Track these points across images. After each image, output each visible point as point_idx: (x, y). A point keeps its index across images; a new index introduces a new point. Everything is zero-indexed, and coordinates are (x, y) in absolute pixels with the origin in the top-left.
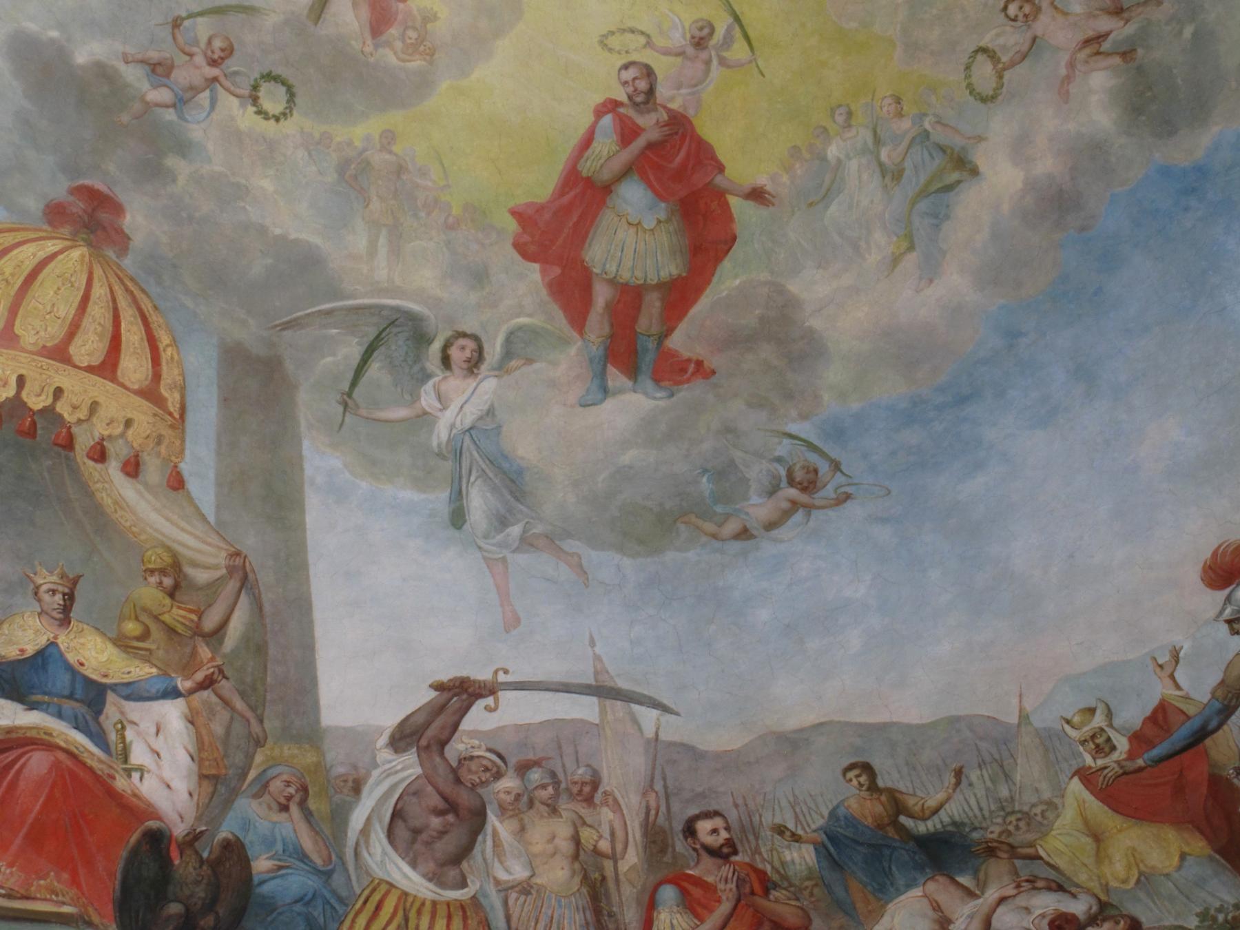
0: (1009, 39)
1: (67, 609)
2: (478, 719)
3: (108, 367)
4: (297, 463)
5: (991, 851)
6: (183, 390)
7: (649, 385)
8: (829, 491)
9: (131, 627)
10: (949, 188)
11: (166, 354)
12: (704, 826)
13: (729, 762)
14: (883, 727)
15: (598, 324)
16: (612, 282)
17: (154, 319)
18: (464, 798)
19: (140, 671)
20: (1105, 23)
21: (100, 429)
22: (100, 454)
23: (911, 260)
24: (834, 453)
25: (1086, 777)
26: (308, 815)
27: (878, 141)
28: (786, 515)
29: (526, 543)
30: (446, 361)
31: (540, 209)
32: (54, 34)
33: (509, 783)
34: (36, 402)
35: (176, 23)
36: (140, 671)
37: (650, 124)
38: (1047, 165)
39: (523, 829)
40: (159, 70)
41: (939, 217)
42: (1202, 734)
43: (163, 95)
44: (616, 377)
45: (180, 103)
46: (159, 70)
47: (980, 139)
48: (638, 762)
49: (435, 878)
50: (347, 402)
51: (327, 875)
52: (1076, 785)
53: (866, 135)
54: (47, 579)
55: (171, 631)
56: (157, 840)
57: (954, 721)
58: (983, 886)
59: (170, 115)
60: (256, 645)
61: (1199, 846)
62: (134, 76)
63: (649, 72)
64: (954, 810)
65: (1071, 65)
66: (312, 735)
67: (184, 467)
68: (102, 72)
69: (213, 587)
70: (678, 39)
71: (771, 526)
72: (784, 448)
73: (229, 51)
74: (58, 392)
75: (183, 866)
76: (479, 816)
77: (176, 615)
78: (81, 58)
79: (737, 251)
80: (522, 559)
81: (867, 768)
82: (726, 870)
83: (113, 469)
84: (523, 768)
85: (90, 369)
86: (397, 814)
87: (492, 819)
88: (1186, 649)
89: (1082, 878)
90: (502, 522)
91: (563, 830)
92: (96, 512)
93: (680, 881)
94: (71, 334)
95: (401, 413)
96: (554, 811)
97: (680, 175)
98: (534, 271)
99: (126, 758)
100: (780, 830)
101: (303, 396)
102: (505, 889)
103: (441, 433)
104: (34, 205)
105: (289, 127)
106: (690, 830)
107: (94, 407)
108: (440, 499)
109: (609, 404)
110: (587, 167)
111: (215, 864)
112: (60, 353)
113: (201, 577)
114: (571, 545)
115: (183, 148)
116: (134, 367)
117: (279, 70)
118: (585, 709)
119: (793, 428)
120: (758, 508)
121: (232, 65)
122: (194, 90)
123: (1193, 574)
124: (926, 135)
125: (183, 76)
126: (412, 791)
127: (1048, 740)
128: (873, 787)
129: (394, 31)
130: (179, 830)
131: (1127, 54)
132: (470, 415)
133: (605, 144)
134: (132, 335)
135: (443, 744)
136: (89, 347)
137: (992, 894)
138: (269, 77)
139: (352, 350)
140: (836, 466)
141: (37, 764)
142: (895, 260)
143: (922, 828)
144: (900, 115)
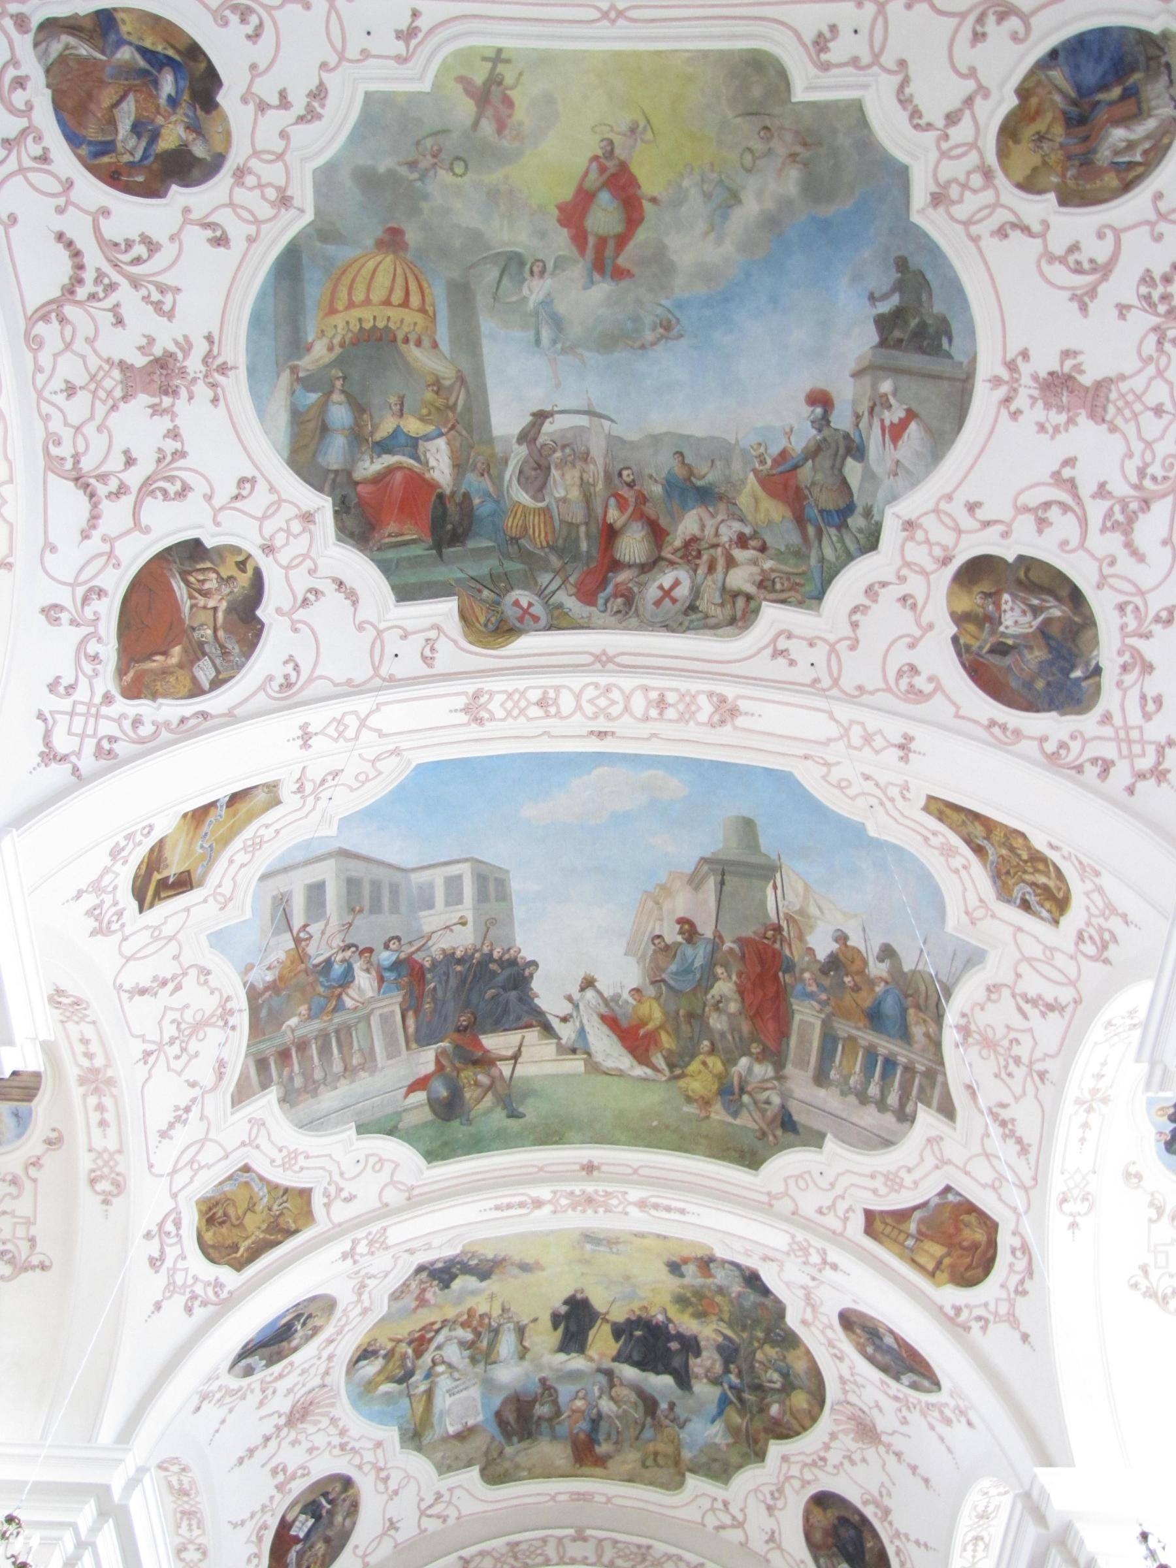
0: (758, 146)
1: (401, 410)
2: (548, 427)
3: (405, 303)
4: (477, 328)
5: (721, 498)
6: (433, 305)
7: (608, 278)
8: (675, 332)
9: (425, 411)
10: (730, 207)
11: (427, 291)
12: (625, 473)
13: (633, 445)
14: (689, 437)
15: (590, 252)
16: (596, 235)
17: (421, 277)
18: (543, 462)
19: (430, 429)
20: (798, 149)
21: (406, 329)
22: (406, 341)
23: (712, 236)
24: (678, 315)
25: (755, 471)
26: (490, 476)
27: (703, 181)
28: (659, 340)
29: (564, 351)
30: (532, 273)
31: (567, 204)
32: (370, 162)
33: (558, 454)
34: (381, 324)
35: (418, 143)
36: (430, 429)
37: (611, 166)
38: (770, 205)
39: (563, 475)
40: (412, 165)
41: (725, 217)
42: (796, 467)
43: (415, 176)
44: (596, 276)
45: (422, 178)
46: (412, 165)
47: (744, 188)
48: (603, 444)
49: (534, 498)
50: (495, 298)
51: (497, 502)
52: (751, 475)
53: (698, 178)
54: (393, 400)
55: (438, 409)
56: (441, 497)
57: (713, 438)
58: (717, 513)
59: (419, 184)
60: (468, 408)
61: (789, 514)
62: (403, 171)
63: (611, 143)
64: (710, 478)
65: (784, 164)
66: (489, 440)
67: (438, 338)
68: (391, 173)
69: (451, 387)
70: (624, 127)
71: (653, 344)
72: (659, 311)
73: (440, 150)
74: (389, 319)
75: (451, 508)
76: (549, 468)
77: (440, 402)
78: (382, 169)
79: (645, 224)
80: (562, 358)
81: (681, 454)
82: (632, 493)
83: (412, 346)
84: (564, 447)
85: (400, 306)
86: (521, 472)
87: (553, 471)
88: (796, 427)
89: (750, 518)
90: (554, 342)
91: (577, 474)
92: (407, 364)
93: (616, 496)
94: (391, 290)
95: (514, 299)
96: (574, 466)
97: (623, 188)
98: (565, 232)
99: (427, 462)
100: (651, 477)
101: (479, 298)
102: (558, 500)
103: (531, 305)
104: (370, 242)
105: (466, 178)
106: (620, 475)
107: (402, 321)
108: (531, 334)
109: (594, 288)
110: (587, 185)
111: (460, 505)
112: (387, 303)
113: (447, 383)
114: (580, 350)
115: (425, 197)
116: (415, 300)
117: (461, 155)
118: (583, 421)
119: (663, 302)
120: (649, 336)
121: (442, 156)
122: (427, 170)
123: (802, 397)
124: (721, 181)
125: (423, 164)
126: (525, 462)
127: (744, 453)
128: (683, 463)
129: (506, 132)
130: (448, 491)
131: (805, 165)
132: (541, 296)
133: (593, 175)
134: (413, 287)
135: (535, 440)
136: (397, 297)
137: (720, 518)
138: (458, 158)
139: (493, 273)
140: (678, 320)
141: (399, 476)
142: (706, 234)
143: (699, 483)
144: (712, 171)
